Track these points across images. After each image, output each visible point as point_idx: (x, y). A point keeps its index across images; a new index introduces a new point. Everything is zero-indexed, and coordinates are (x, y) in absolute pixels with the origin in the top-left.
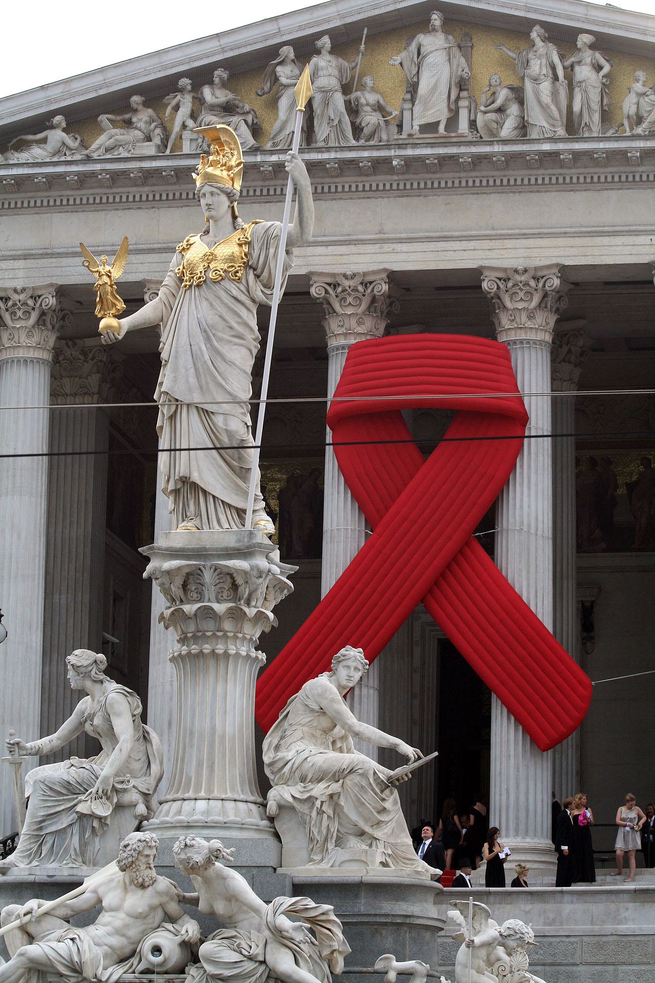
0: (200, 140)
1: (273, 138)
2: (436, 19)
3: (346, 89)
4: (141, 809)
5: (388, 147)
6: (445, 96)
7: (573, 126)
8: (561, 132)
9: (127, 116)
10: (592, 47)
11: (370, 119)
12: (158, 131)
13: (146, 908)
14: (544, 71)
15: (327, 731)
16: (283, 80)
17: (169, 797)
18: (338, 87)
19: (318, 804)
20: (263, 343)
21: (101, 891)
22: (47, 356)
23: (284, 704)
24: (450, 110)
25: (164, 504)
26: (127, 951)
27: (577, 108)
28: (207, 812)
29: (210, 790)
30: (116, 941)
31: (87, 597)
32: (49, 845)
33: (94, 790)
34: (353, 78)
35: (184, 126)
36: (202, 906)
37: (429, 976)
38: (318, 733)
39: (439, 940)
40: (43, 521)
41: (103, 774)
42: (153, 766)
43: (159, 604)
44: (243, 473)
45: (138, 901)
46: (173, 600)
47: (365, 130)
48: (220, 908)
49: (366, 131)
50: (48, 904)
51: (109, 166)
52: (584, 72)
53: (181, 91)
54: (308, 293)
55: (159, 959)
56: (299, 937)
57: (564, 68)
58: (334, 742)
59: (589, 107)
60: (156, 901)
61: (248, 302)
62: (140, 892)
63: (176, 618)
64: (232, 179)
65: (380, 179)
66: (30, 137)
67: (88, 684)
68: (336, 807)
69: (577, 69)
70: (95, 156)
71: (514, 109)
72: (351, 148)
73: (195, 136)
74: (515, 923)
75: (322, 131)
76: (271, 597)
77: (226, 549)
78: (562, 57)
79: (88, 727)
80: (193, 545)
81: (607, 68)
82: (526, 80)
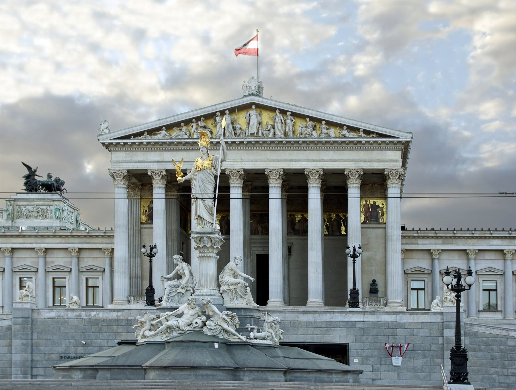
1: (216, 135)
3: (232, 124)
4: (192, 291)
5: (243, 138)
6: (256, 126)
7: (286, 135)
8: (283, 136)
11: (238, 131)
12: (188, 132)
13: (194, 314)
14: (279, 121)
15: (234, 274)
16: (218, 121)
17: (198, 289)
18: (231, 123)
19: (232, 290)
20: (216, 185)
21: (183, 310)
22: (164, 186)
23: (223, 268)
24: (257, 130)
25: (194, 222)
26: (190, 323)
27: (287, 130)
28: (207, 292)
29: (207, 287)
30: (187, 321)
31: (176, 243)
32: (171, 299)
33: (181, 287)
34: (234, 121)
35: (194, 131)
36: (207, 313)
37: (257, 329)
38: (231, 275)
39: (260, 321)
40: (165, 225)
41: (183, 283)
42: (194, 281)
43: (193, 244)
44: (213, 215)
45: (192, 312)
46: (197, 244)
47: (237, 134)
48: (211, 313)
50: (171, 313)
52: (288, 121)
54: (225, 173)
55: (197, 325)
56: (228, 320)
57: (284, 120)
58: (235, 277)
59: (290, 130)
60: (196, 312)
61: (212, 175)
62: (192, 310)
63: (198, 248)
64: (207, 144)
65: (241, 146)
67: (178, 263)
68: (236, 290)
69: (287, 120)
70: (173, 138)
71: (272, 130)
72: (234, 139)
73: (197, 134)
74: (277, 318)
75: (227, 134)
76: (220, 244)
79: (179, 272)
80: (202, 231)
81: (294, 121)
82: (275, 123)
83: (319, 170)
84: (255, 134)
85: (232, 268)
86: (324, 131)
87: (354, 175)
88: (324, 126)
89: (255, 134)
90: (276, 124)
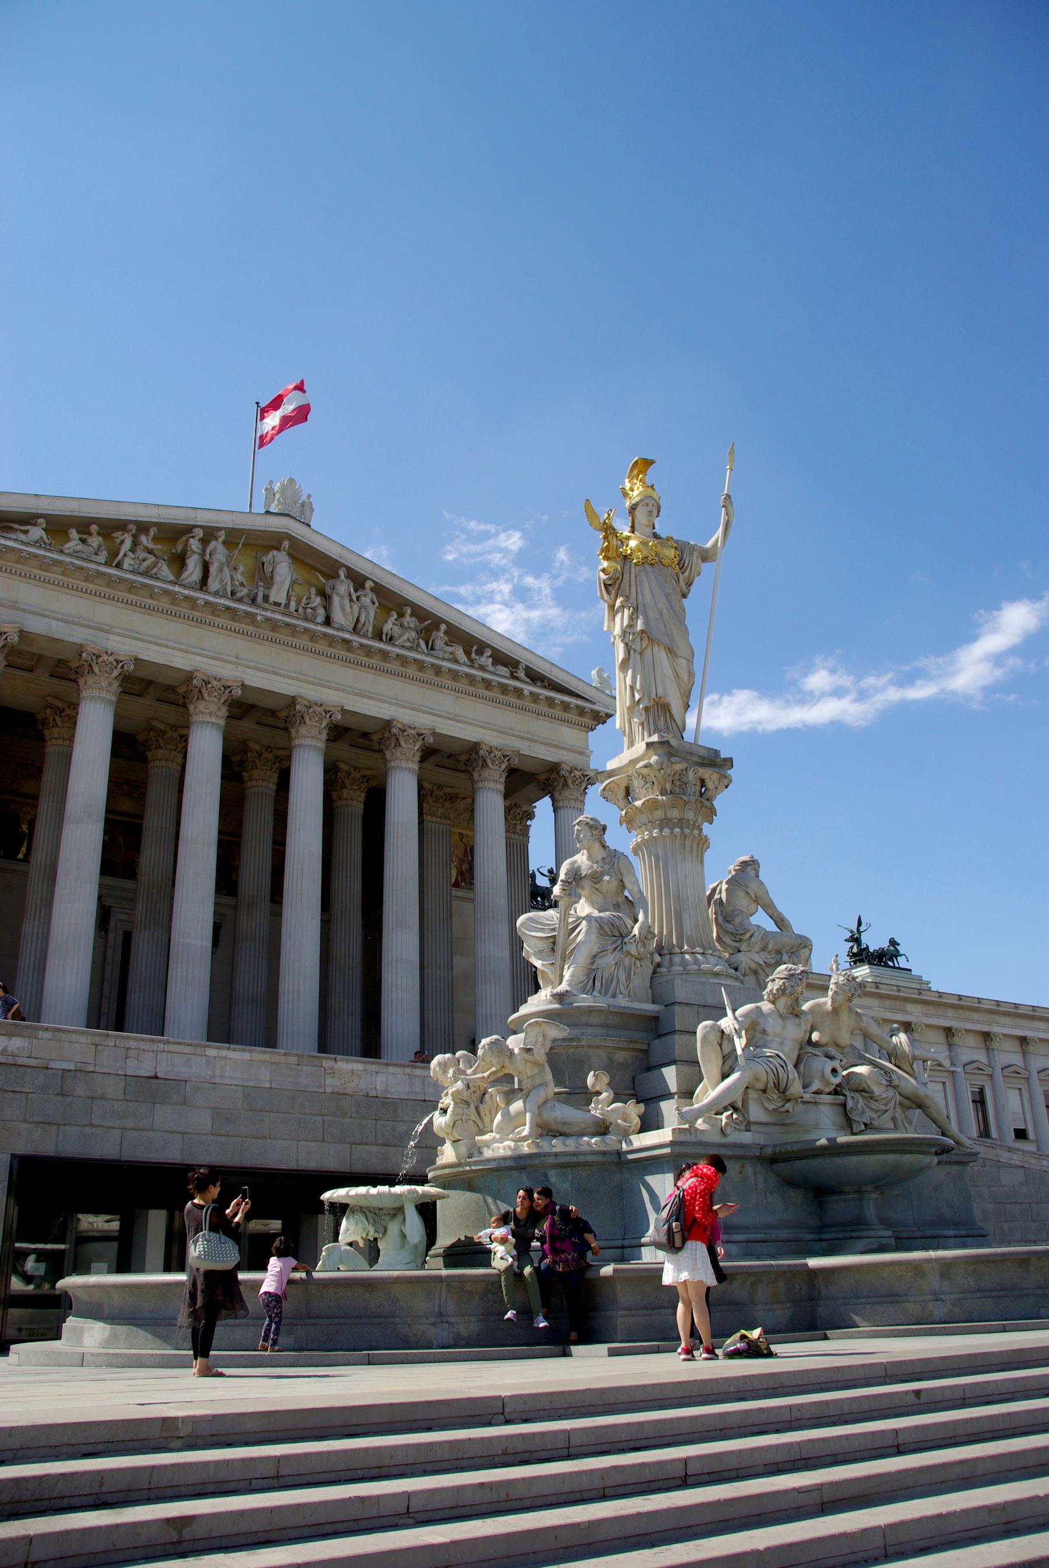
0: (136, 566)
2: (286, 544)
7: (355, 630)
9: (84, 536)
10: (372, 589)
16: (194, 548)
27: (362, 619)
35: (125, 555)
49: (239, 595)
51: (76, 562)
52: (366, 600)
53: (128, 531)
66: (16, 526)
69: (363, 599)
70: (66, 551)
73: (132, 562)
75: (213, 584)
77: (703, 758)
78: (356, 591)
83: (423, 732)
84: (283, 606)
85: (758, 895)
86: (439, 644)
87: (497, 762)
88: (441, 634)
89: (283, 606)
90: (336, 600)
